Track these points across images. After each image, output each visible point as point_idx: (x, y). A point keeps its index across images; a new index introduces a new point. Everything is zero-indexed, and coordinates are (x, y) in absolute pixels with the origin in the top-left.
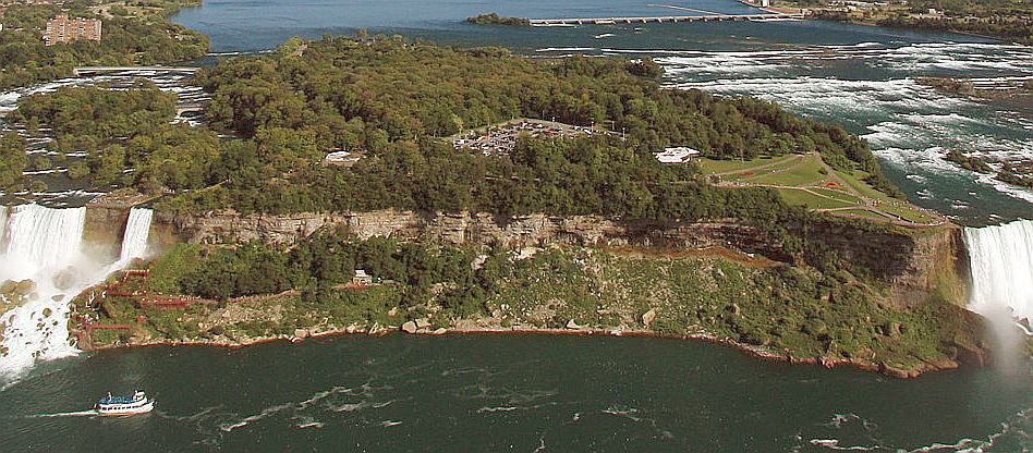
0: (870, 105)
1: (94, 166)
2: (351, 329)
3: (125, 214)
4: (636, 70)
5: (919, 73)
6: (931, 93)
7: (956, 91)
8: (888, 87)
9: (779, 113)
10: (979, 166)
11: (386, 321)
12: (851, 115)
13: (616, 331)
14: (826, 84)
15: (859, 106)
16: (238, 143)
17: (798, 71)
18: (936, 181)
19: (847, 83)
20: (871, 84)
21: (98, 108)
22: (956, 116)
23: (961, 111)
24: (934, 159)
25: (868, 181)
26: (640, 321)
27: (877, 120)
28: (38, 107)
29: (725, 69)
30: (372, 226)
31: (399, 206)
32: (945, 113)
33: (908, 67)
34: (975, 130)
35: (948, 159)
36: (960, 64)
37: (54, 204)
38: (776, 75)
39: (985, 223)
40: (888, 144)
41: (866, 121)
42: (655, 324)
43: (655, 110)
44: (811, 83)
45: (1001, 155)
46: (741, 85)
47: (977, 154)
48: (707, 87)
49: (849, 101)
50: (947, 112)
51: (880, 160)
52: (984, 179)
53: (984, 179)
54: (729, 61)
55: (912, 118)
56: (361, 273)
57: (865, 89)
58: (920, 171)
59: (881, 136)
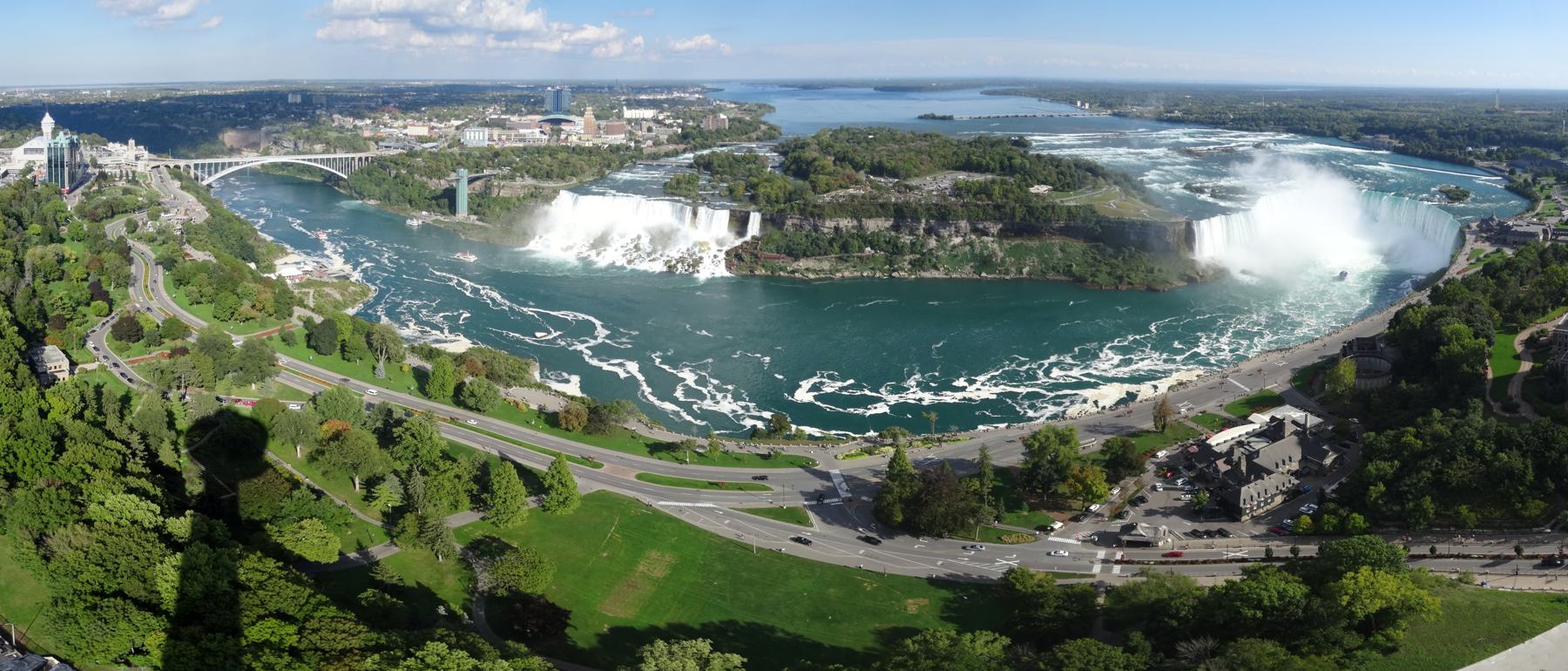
0: (1144, 162)
1: (731, 191)
2: (865, 274)
3: (748, 214)
4: (1016, 143)
5: (1171, 145)
6: (1176, 154)
7: (1190, 153)
8: (1154, 152)
9: (1096, 166)
10: (1201, 190)
11: (883, 271)
12: (1134, 167)
13: (1008, 277)
14: (1121, 150)
15: (1137, 162)
16: (800, 182)
17: (1104, 143)
18: (1179, 198)
19: (1132, 150)
20: (1145, 151)
21: (733, 163)
22: (1188, 166)
23: (1192, 164)
24: (1177, 188)
25: (1143, 200)
26: (1021, 273)
27: (1148, 169)
28: (702, 161)
29: (1063, 142)
30: (873, 225)
31: (887, 217)
32: (1184, 164)
33: (1164, 141)
34: (1197, 173)
35: (1185, 188)
36: (1192, 140)
37: (714, 208)
38: (1093, 146)
39: (1202, 218)
40: (1153, 181)
41: (1142, 170)
42: (1030, 273)
43: (1028, 166)
44: (1112, 150)
45: (1210, 184)
46: (1074, 151)
47: (1198, 185)
48: (1055, 152)
49: (1133, 160)
50: (1184, 164)
51: (1151, 190)
52: (1203, 197)
53: (1203, 197)
54: (1068, 138)
55: (1167, 168)
56: (869, 249)
57: (1142, 153)
58: (1173, 195)
59: (1150, 177)
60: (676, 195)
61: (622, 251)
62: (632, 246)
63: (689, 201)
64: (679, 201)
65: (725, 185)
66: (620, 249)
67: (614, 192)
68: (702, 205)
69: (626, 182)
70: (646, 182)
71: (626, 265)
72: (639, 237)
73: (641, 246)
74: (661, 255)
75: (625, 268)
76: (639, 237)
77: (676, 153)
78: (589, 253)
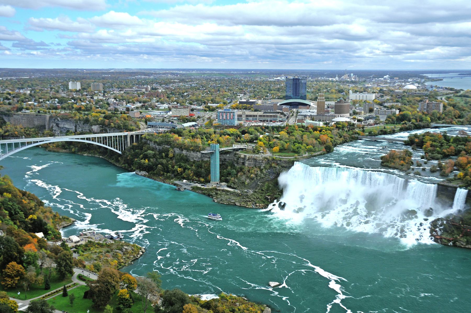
60: (390, 168)
61: (343, 215)
62: (351, 211)
63: (402, 174)
64: (393, 174)
65: (436, 162)
66: (341, 213)
67: (338, 164)
68: (414, 178)
69: (347, 155)
70: (363, 156)
71: (345, 226)
72: (358, 203)
73: (359, 211)
74: (374, 219)
75: (345, 229)
76: (358, 203)
77: (393, 132)
78: (316, 215)
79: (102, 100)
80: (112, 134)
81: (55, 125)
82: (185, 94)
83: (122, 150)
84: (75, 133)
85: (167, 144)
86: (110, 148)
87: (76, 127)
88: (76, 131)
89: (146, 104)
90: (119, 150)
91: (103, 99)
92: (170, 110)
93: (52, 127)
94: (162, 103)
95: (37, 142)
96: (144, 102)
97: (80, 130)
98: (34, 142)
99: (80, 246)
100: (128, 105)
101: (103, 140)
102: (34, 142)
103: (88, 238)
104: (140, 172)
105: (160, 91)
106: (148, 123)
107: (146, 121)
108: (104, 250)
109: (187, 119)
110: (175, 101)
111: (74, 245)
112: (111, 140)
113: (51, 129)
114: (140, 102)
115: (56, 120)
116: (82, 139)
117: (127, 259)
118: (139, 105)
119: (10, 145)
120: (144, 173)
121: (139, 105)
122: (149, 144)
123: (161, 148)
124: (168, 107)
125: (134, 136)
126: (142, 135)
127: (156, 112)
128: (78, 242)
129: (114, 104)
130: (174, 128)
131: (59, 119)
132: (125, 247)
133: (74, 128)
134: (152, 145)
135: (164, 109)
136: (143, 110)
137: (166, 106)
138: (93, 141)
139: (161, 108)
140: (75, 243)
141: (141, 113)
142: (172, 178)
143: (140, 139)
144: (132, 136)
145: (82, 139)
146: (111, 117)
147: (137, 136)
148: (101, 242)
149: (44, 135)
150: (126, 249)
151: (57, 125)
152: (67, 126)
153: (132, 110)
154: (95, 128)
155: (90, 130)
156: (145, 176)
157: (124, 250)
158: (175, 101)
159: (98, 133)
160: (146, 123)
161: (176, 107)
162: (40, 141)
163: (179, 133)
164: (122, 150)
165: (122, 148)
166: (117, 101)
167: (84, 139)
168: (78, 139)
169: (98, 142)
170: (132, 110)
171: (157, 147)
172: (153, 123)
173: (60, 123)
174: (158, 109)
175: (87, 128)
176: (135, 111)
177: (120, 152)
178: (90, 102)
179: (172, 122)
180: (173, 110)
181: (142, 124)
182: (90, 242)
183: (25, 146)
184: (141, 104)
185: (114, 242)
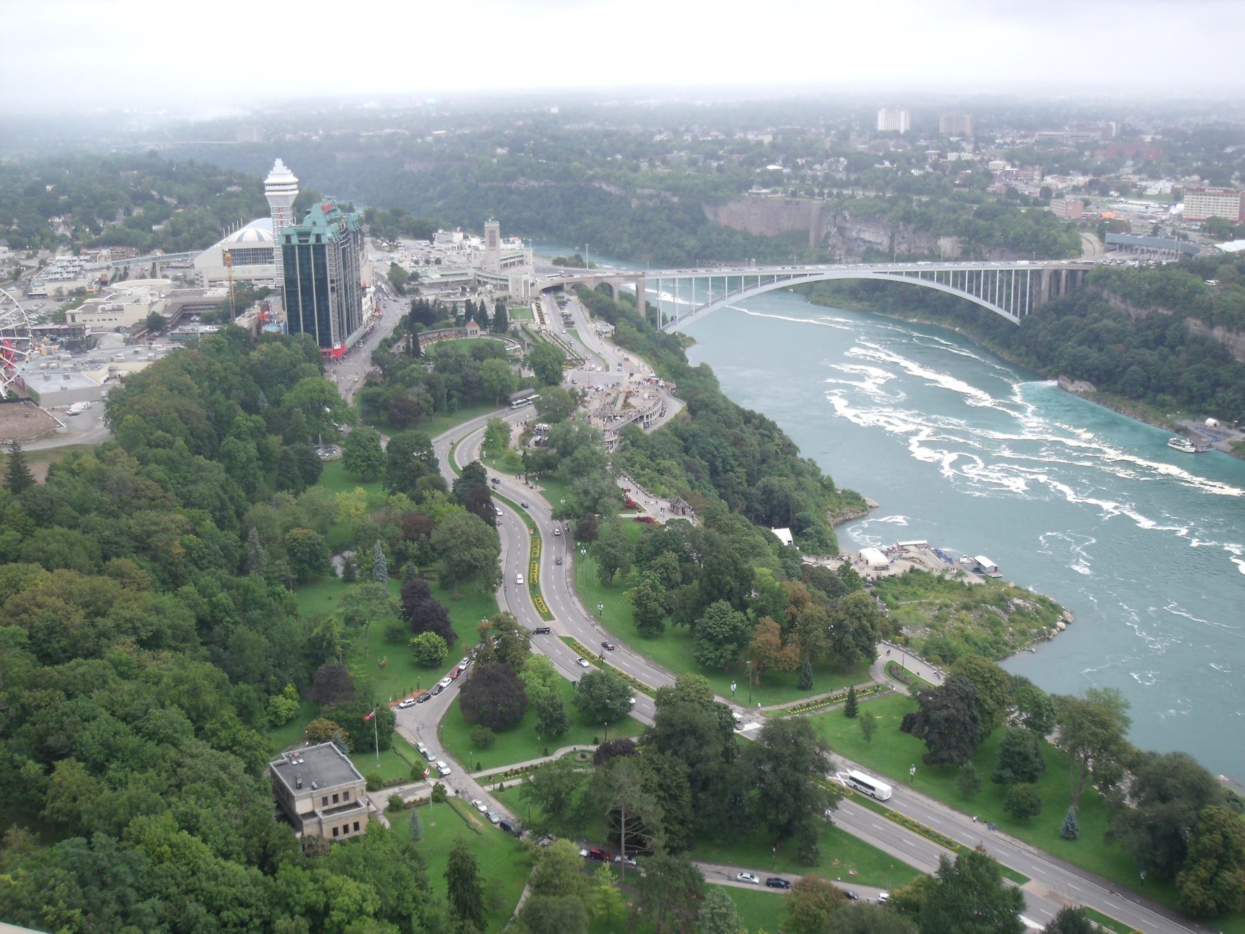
79: (969, 164)
80: (995, 265)
81: (834, 230)
82: (1229, 150)
83: (1023, 312)
84: (890, 257)
85: (1163, 305)
86: (987, 305)
87: (892, 238)
88: (891, 249)
89: (1102, 179)
90: (1015, 313)
91: (972, 161)
92: (1177, 197)
93: (828, 235)
94: (1155, 176)
95: (788, 277)
96: (1099, 172)
97: (904, 247)
98: (781, 278)
99: (886, 580)
100: (1049, 180)
101: (970, 281)
102: (781, 278)
103: (911, 559)
104: (1072, 382)
105: (1148, 139)
106: (1109, 236)
107: (1103, 229)
108: (956, 600)
109: (1232, 230)
110: (1197, 171)
111: (874, 574)
112: (994, 283)
113: (823, 243)
114: (1085, 173)
115: (839, 219)
116: (909, 274)
117: (1018, 637)
118: (1081, 180)
119: (718, 281)
120: (1083, 386)
121: (1081, 180)
122: (1107, 301)
123: (1144, 314)
124: (1173, 190)
125: (1064, 273)
126: (1085, 272)
127: (1135, 205)
128: (885, 568)
129: (1008, 174)
130: (1191, 256)
131: (847, 214)
132: (1017, 601)
133: (886, 241)
134: (1115, 302)
135: (1159, 197)
136: (1094, 197)
137: (1165, 186)
138: (939, 280)
139: (1149, 192)
140: (876, 568)
141: (1087, 203)
142: (1173, 410)
143: (1079, 283)
144: (1056, 273)
145: (909, 274)
146: (996, 216)
147: (1072, 273)
148: (948, 577)
149: (803, 260)
150: (1017, 606)
151: (841, 230)
152: (867, 236)
153: (1060, 196)
154: (946, 244)
155: (931, 251)
156: (1086, 395)
157: (1013, 608)
158: (1197, 171)
159: (956, 260)
160: (1102, 237)
161: (1200, 191)
162: (795, 276)
163: (1206, 269)
164: (1023, 312)
165: (1023, 306)
166: (1013, 166)
167: (915, 274)
168: (900, 273)
169: (955, 285)
170: (1060, 196)
171: (1132, 310)
172: (1123, 237)
173: (848, 225)
174: (1140, 195)
175: (923, 244)
176: (1069, 198)
177: (1015, 320)
178: (935, 166)
179: (1185, 237)
180: (1187, 198)
181: (1090, 241)
182: (918, 572)
183: (756, 286)
184: (1087, 179)
185: (983, 582)
